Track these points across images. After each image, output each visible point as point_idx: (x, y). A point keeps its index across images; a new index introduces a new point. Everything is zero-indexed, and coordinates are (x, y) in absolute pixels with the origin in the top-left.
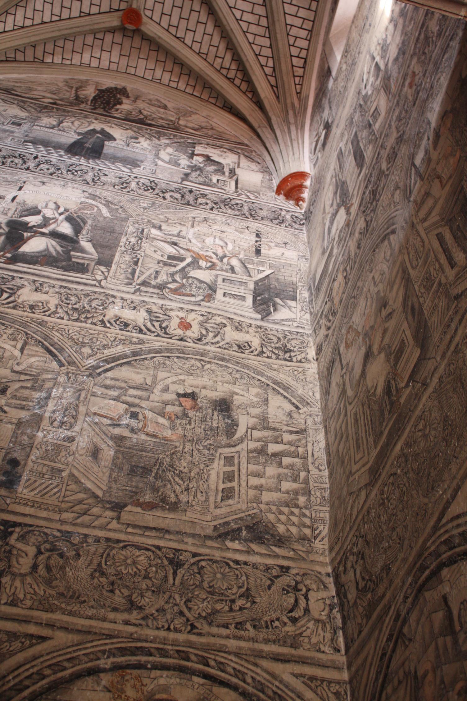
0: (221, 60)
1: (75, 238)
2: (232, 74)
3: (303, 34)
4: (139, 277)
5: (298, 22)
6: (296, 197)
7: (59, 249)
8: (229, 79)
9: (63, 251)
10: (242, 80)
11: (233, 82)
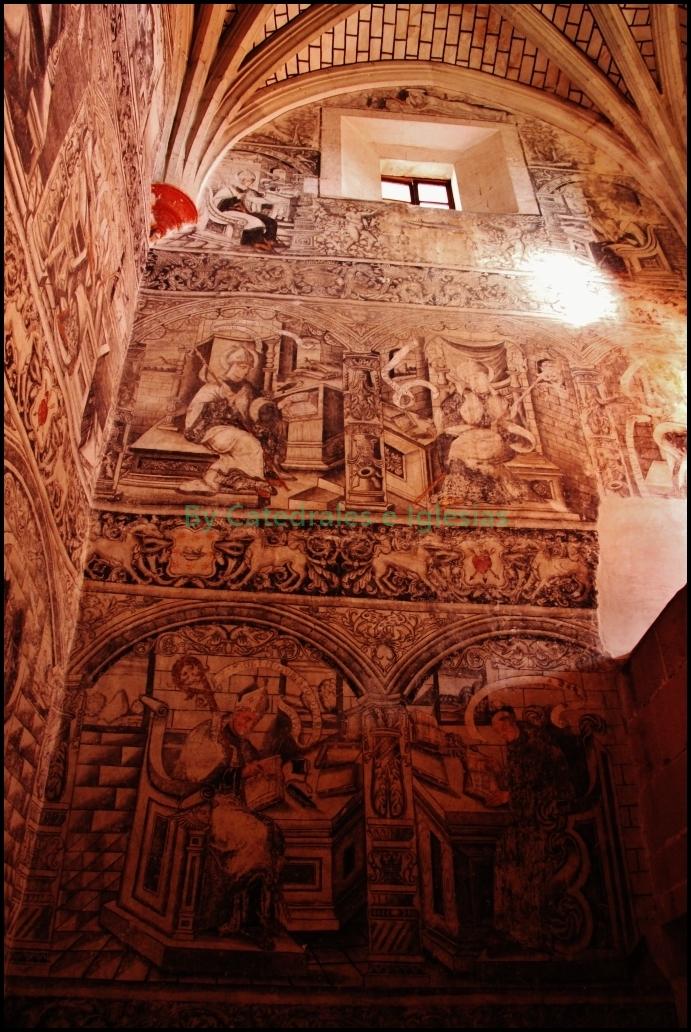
3: (327, 58)
5: (339, 44)
6: (163, 223)
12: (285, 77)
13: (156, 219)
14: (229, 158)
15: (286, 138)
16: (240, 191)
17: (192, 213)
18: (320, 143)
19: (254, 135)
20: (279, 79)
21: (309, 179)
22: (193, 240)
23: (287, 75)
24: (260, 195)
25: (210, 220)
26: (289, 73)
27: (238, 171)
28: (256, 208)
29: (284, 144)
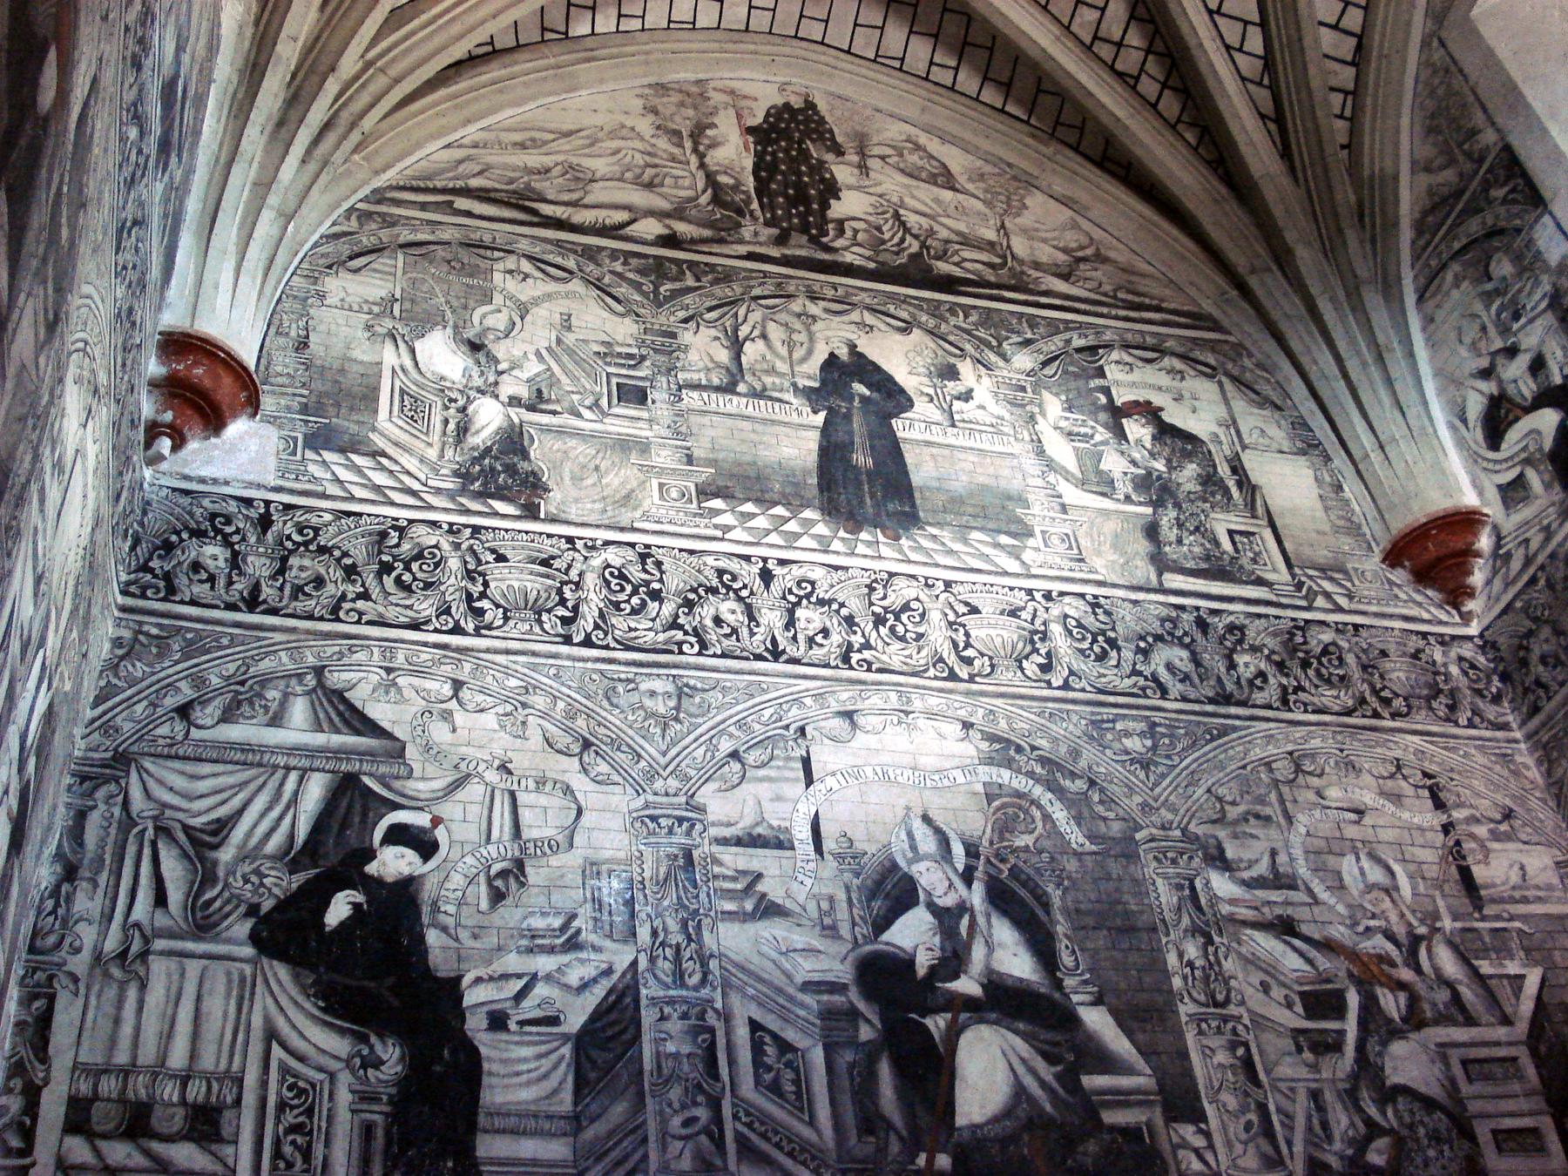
0: (1097, 14)
1: (1057, 995)
2: (1130, 61)
4: (1289, 1143)
6: (1451, 586)
7: (1047, 1072)
8: (1120, 75)
9: (1058, 1077)
10: (1164, 86)
11: (1134, 88)
12: (1350, 72)
13: (1440, 590)
14: (1428, 321)
15: (1449, 175)
16: (1486, 374)
17: (1467, 521)
18: (1493, 124)
19: (1419, 227)
20: (1351, 86)
21: (1538, 227)
22: (1509, 555)
23: (1352, 64)
24: (1512, 352)
25: (1499, 487)
26: (1349, 58)
27: (1453, 335)
28: (1528, 389)
29: (1459, 194)
